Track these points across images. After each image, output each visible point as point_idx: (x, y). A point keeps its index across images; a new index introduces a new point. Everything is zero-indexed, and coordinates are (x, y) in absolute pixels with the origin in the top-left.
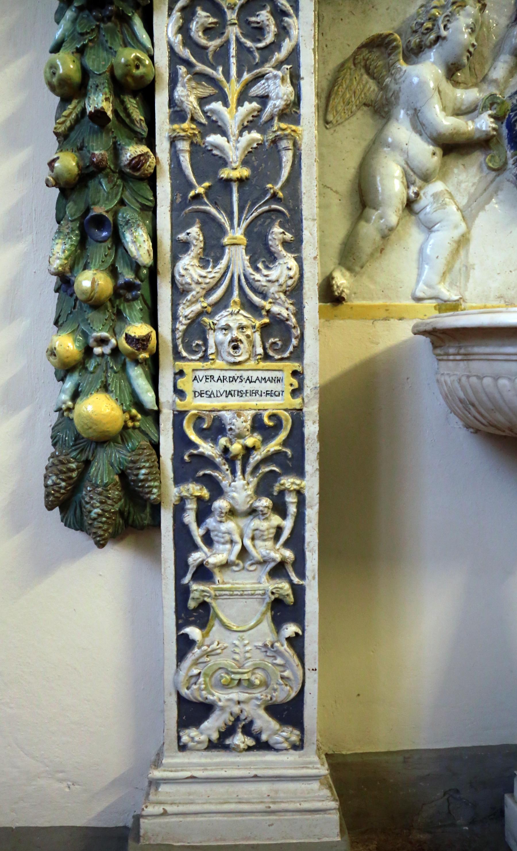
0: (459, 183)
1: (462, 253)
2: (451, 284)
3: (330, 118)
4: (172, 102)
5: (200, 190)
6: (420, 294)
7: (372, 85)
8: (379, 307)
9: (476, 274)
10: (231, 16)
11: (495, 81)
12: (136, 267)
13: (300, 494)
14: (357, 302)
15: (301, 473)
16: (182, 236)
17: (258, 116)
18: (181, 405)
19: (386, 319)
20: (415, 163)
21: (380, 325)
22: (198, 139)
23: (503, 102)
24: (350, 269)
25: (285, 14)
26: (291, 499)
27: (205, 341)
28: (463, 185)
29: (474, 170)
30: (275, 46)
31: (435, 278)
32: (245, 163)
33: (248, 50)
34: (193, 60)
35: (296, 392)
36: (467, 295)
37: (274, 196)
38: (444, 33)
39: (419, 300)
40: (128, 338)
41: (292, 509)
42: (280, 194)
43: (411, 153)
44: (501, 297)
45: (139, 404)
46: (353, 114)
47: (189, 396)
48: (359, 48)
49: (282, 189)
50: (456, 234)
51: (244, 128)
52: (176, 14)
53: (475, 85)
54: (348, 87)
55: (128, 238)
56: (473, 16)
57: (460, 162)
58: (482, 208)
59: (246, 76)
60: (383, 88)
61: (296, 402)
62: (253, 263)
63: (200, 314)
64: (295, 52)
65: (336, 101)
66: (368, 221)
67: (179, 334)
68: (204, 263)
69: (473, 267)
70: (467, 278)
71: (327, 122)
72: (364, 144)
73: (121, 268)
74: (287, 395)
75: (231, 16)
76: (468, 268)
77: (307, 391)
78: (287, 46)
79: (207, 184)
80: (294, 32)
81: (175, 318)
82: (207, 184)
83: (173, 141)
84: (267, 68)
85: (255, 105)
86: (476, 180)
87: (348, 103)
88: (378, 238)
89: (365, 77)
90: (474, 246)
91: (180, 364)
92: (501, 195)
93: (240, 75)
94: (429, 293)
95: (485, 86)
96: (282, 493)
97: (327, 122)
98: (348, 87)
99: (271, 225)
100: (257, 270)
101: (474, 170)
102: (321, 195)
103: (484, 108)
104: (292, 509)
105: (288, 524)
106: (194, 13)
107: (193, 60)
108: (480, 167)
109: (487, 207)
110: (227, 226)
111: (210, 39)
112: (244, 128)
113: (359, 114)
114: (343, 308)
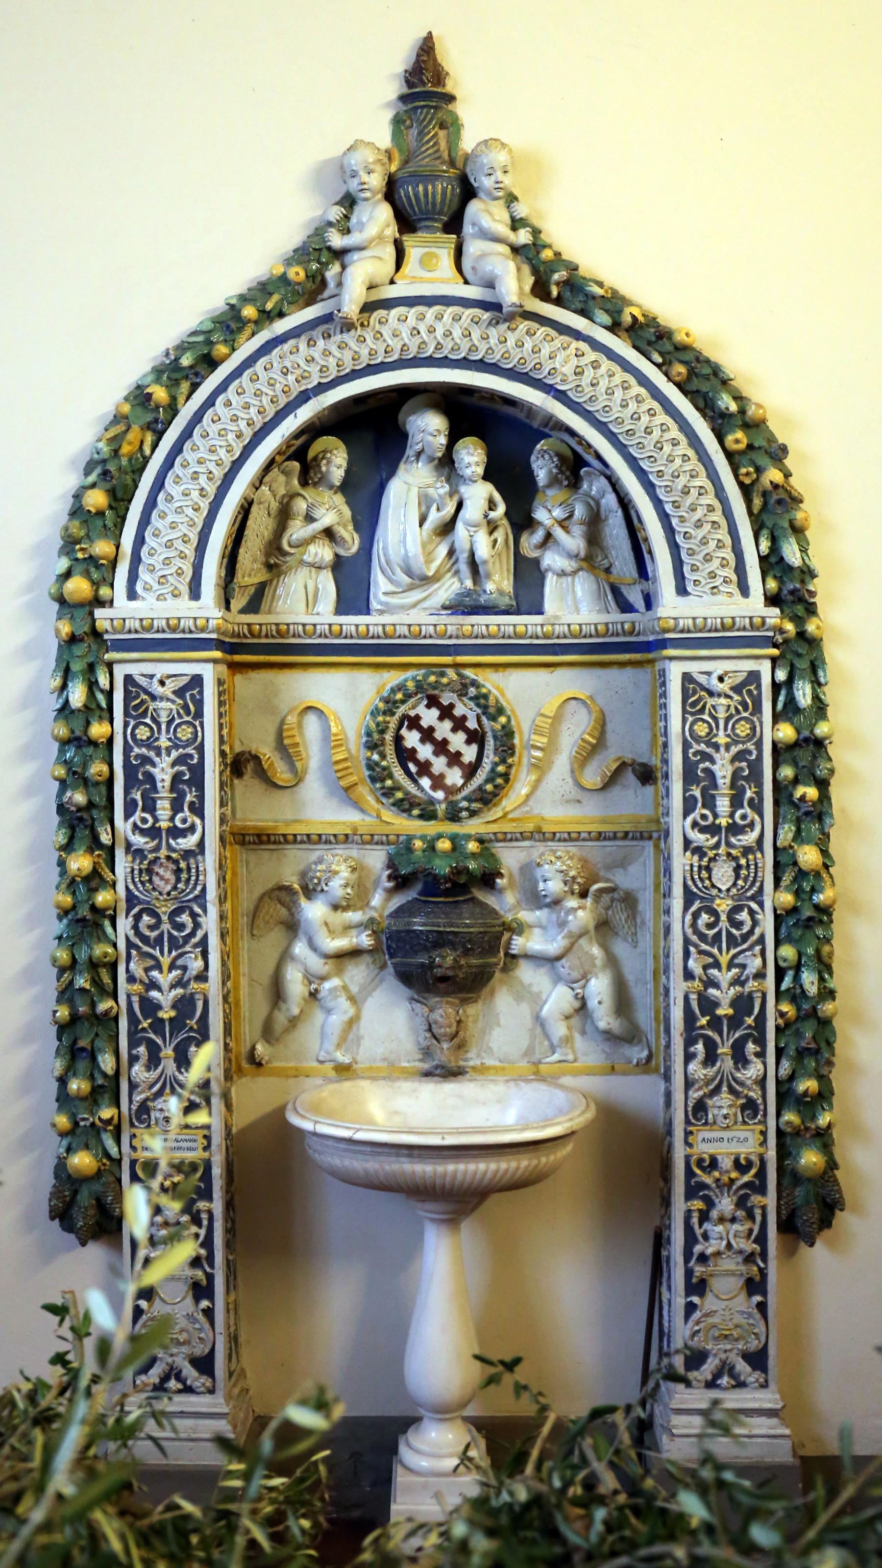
0: (352, 977)
1: (354, 1028)
2: (346, 1051)
3: (255, 932)
4: (127, 970)
5: (145, 1025)
6: (321, 1058)
7: (284, 912)
8: (291, 1068)
9: (366, 1043)
10: (165, 918)
11: (374, 908)
12: (105, 1075)
13: (210, 1213)
14: (276, 1064)
15: (210, 1199)
16: (134, 1052)
17: (182, 978)
18: (134, 1155)
19: (296, 1076)
20: (311, 971)
21: (291, 1081)
22: (144, 994)
23: (379, 923)
24: (268, 1042)
25: (199, 916)
26: (204, 1216)
27: (149, 1117)
28: (356, 978)
29: (363, 967)
30: (193, 934)
31: (331, 1048)
32: (174, 1007)
33: (176, 938)
34: (140, 944)
35: (207, 1148)
36: (359, 1058)
37: (191, 1029)
38: (326, 888)
39: (322, 1062)
40: (100, 1118)
41: (205, 1222)
42: (195, 1027)
43: (309, 965)
44: (385, 1059)
45: (107, 1155)
46: (272, 929)
47: (139, 1150)
48: (273, 890)
49: (197, 1023)
50: (346, 1017)
51: (173, 986)
52: (131, 919)
53: (361, 908)
54: (267, 913)
55: (100, 1058)
56: (345, 878)
57: (353, 961)
58: (370, 994)
59: (174, 954)
60: (292, 915)
61: (206, 1155)
62: (179, 1069)
63: (147, 1099)
64: (206, 936)
65: (259, 922)
66: (279, 1009)
67: (133, 1112)
68: (148, 1069)
69: (362, 1037)
70: (359, 1045)
71: (253, 935)
72: (280, 950)
73: (97, 1075)
74: (200, 1150)
75: (165, 918)
76: (359, 1039)
77: (214, 1147)
78: (200, 934)
79: (149, 1021)
80: (204, 927)
81: (131, 1101)
82: (149, 1021)
83: (129, 996)
84: (188, 948)
85: (179, 972)
86: (365, 974)
87: (268, 923)
88: (286, 1022)
89: (279, 906)
90: (364, 1022)
91: (134, 1130)
92: (384, 985)
93: (170, 952)
94: (328, 1058)
95: (367, 910)
96: (199, 1211)
97: (253, 935)
98: (267, 913)
99: (189, 1046)
100: (181, 1073)
101: (363, 967)
102: (250, 985)
103: (366, 927)
104: (205, 1222)
105: (203, 1232)
106: (141, 917)
107: (140, 944)
108: (368, 965)
109: (374, 994)
110: (162, 1046)
111: (152, 931)
112: (173, 986)
113: (276, 929)
114: (262, 1069)
